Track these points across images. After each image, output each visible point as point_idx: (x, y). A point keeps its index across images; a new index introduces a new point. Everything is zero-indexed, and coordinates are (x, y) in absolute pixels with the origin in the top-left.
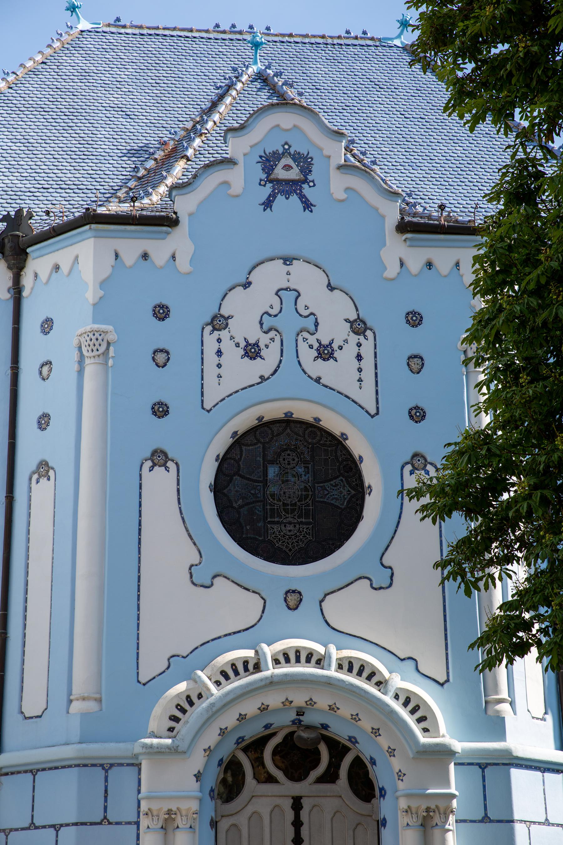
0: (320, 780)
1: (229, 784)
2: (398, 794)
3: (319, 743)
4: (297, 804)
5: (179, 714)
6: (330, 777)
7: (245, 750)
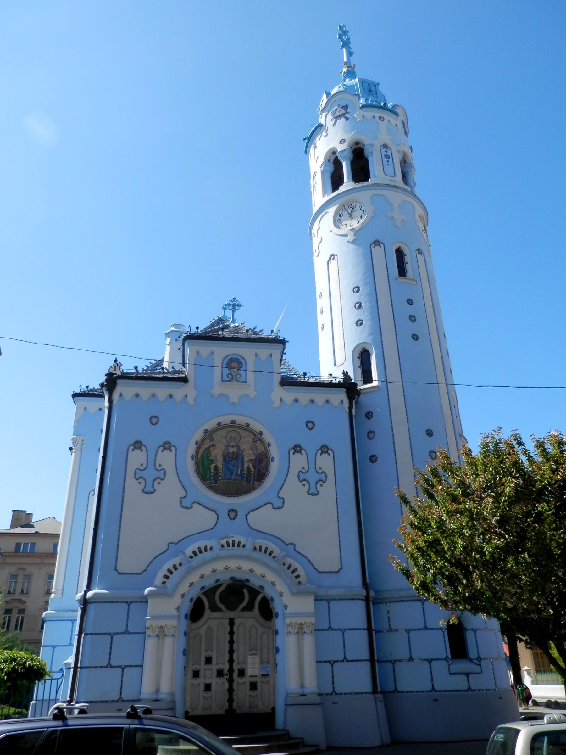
0: (244, 610)
1: (196, 612)
2: (286, 615)
3: (243, 589)
4: (232, 623)
5: (169, 575)
6: (249, 608)
7: (205, 594)
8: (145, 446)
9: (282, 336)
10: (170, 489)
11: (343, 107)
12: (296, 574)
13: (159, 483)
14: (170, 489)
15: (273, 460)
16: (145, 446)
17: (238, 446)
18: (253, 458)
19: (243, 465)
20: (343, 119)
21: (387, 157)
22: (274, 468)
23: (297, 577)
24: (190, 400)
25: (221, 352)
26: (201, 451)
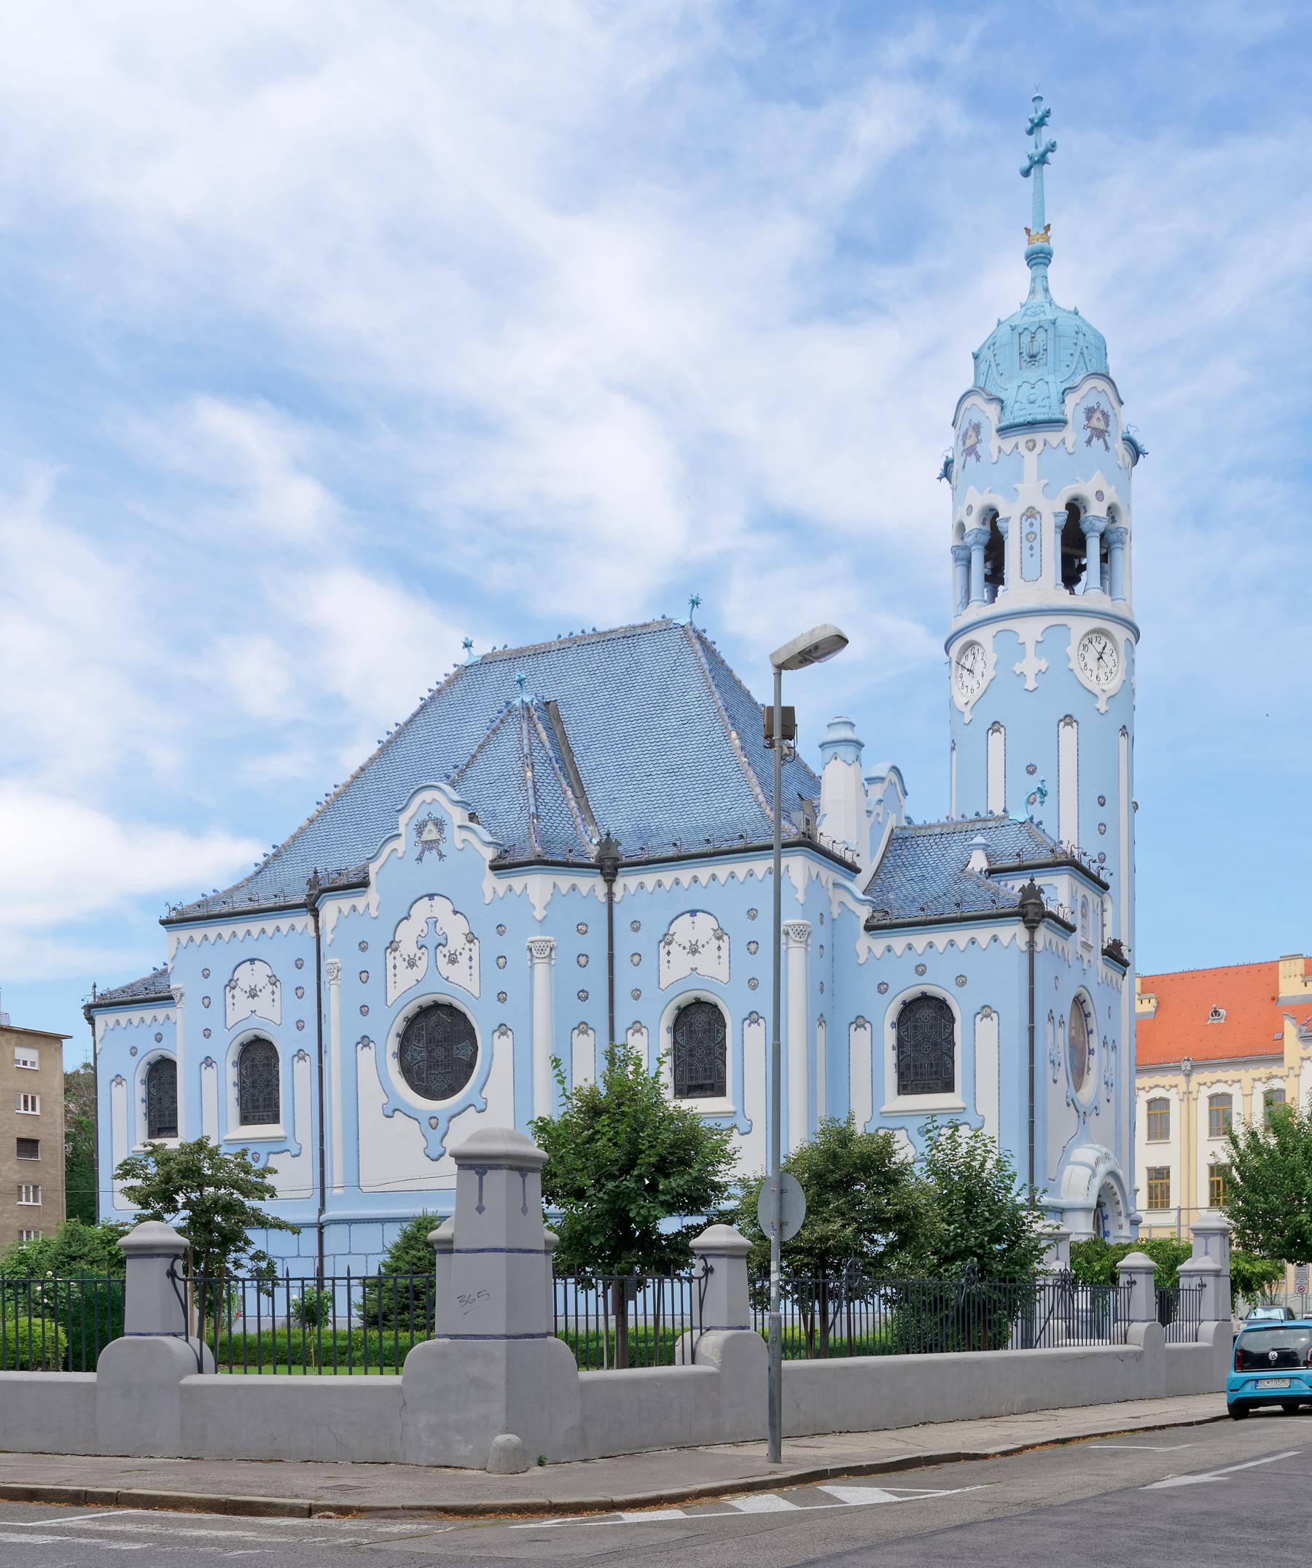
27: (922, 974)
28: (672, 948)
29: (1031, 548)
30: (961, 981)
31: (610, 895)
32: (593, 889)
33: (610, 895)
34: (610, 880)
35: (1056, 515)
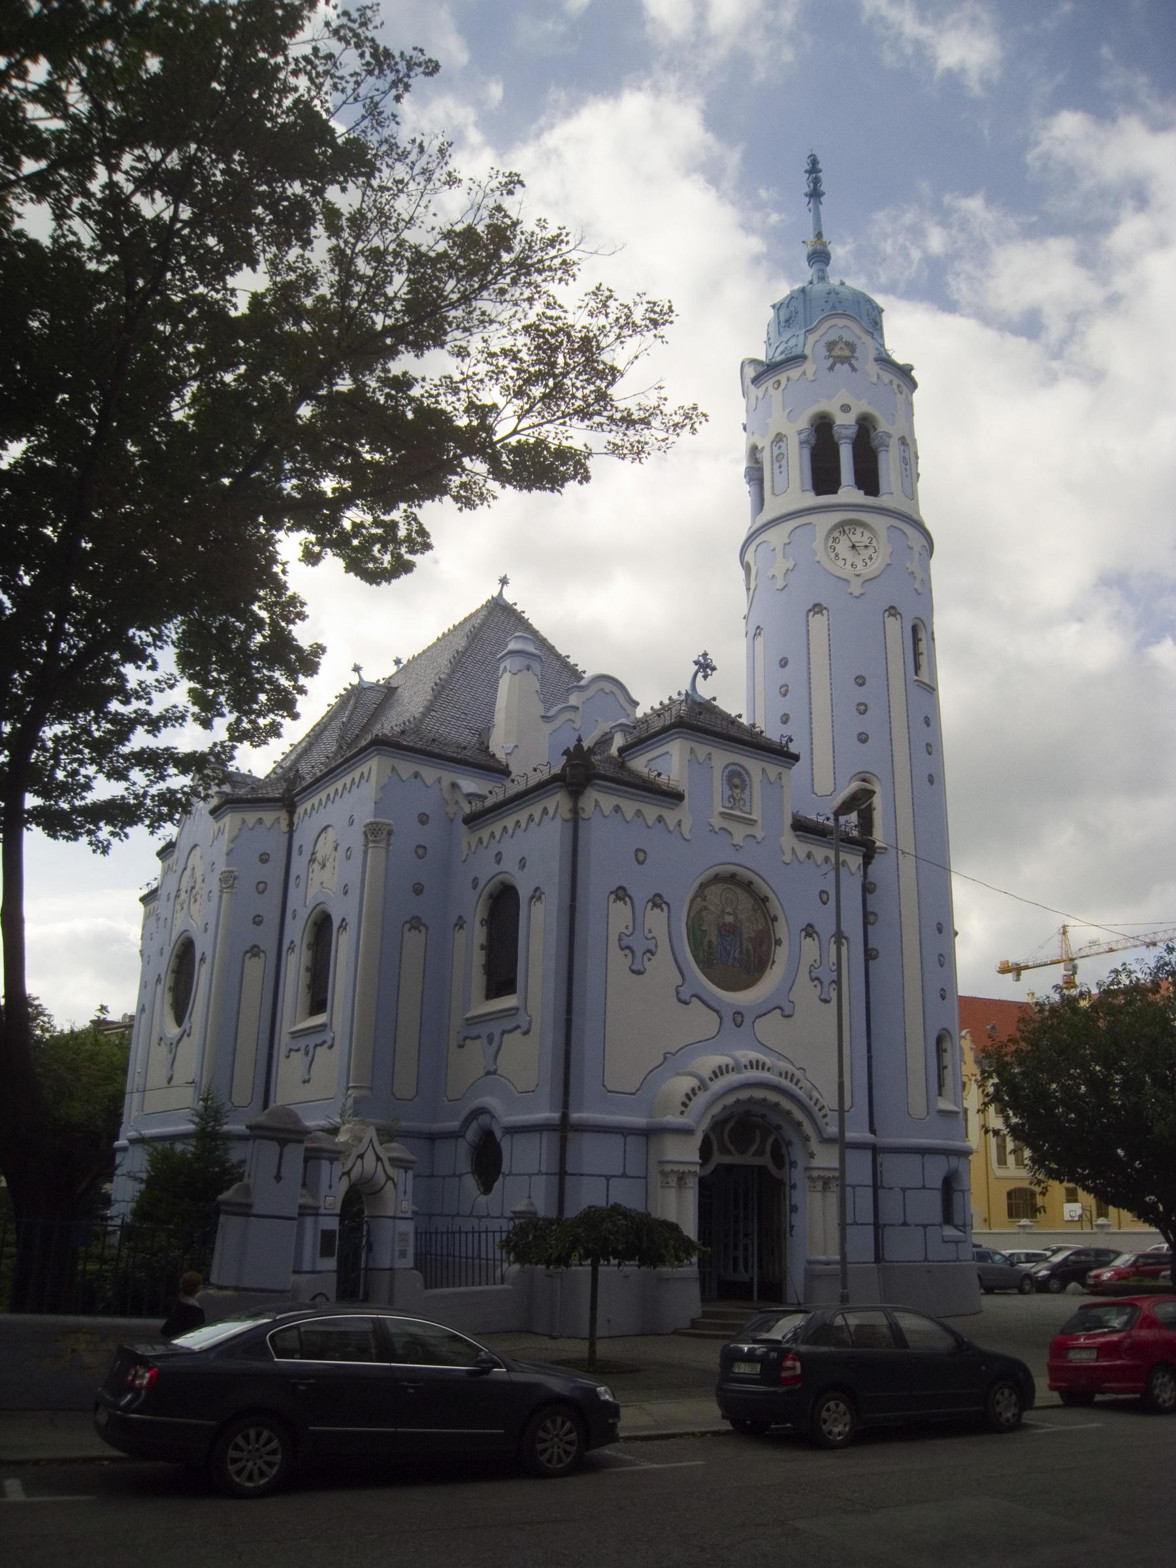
8: (631, 898)
9: (793, 748)
10: (661, 968)
11: (847, 344)
12: (823, 1112)
13: (650, 960)
14: (661, 968)
15: (778, 942)
16: (631, 898)
17: (736, 916)
18: (753, 935)
19: (741, 944)
20: (846, 366)
21: (904, 458)
22: (781, 955)
23: (825, 1116)
24: (686, 829)
25: (721, 758)
26: (692, 915)
27: (498, 862)
28: (316, 866)
29: (780, 467)
30: (523, 864)
31: (291, 824)
32: (278, 820)
33: (291, 824)
34: (291, 811)
35: (800, 433)
